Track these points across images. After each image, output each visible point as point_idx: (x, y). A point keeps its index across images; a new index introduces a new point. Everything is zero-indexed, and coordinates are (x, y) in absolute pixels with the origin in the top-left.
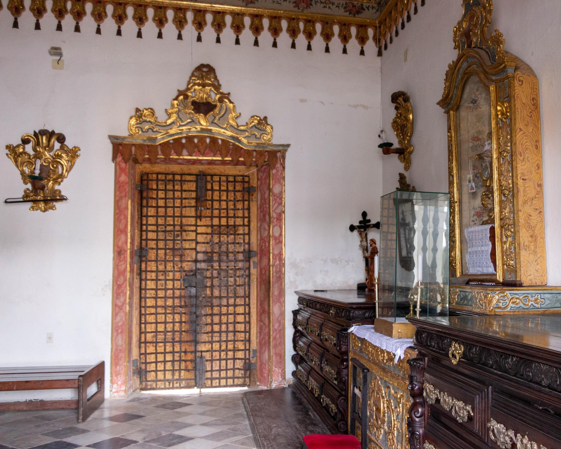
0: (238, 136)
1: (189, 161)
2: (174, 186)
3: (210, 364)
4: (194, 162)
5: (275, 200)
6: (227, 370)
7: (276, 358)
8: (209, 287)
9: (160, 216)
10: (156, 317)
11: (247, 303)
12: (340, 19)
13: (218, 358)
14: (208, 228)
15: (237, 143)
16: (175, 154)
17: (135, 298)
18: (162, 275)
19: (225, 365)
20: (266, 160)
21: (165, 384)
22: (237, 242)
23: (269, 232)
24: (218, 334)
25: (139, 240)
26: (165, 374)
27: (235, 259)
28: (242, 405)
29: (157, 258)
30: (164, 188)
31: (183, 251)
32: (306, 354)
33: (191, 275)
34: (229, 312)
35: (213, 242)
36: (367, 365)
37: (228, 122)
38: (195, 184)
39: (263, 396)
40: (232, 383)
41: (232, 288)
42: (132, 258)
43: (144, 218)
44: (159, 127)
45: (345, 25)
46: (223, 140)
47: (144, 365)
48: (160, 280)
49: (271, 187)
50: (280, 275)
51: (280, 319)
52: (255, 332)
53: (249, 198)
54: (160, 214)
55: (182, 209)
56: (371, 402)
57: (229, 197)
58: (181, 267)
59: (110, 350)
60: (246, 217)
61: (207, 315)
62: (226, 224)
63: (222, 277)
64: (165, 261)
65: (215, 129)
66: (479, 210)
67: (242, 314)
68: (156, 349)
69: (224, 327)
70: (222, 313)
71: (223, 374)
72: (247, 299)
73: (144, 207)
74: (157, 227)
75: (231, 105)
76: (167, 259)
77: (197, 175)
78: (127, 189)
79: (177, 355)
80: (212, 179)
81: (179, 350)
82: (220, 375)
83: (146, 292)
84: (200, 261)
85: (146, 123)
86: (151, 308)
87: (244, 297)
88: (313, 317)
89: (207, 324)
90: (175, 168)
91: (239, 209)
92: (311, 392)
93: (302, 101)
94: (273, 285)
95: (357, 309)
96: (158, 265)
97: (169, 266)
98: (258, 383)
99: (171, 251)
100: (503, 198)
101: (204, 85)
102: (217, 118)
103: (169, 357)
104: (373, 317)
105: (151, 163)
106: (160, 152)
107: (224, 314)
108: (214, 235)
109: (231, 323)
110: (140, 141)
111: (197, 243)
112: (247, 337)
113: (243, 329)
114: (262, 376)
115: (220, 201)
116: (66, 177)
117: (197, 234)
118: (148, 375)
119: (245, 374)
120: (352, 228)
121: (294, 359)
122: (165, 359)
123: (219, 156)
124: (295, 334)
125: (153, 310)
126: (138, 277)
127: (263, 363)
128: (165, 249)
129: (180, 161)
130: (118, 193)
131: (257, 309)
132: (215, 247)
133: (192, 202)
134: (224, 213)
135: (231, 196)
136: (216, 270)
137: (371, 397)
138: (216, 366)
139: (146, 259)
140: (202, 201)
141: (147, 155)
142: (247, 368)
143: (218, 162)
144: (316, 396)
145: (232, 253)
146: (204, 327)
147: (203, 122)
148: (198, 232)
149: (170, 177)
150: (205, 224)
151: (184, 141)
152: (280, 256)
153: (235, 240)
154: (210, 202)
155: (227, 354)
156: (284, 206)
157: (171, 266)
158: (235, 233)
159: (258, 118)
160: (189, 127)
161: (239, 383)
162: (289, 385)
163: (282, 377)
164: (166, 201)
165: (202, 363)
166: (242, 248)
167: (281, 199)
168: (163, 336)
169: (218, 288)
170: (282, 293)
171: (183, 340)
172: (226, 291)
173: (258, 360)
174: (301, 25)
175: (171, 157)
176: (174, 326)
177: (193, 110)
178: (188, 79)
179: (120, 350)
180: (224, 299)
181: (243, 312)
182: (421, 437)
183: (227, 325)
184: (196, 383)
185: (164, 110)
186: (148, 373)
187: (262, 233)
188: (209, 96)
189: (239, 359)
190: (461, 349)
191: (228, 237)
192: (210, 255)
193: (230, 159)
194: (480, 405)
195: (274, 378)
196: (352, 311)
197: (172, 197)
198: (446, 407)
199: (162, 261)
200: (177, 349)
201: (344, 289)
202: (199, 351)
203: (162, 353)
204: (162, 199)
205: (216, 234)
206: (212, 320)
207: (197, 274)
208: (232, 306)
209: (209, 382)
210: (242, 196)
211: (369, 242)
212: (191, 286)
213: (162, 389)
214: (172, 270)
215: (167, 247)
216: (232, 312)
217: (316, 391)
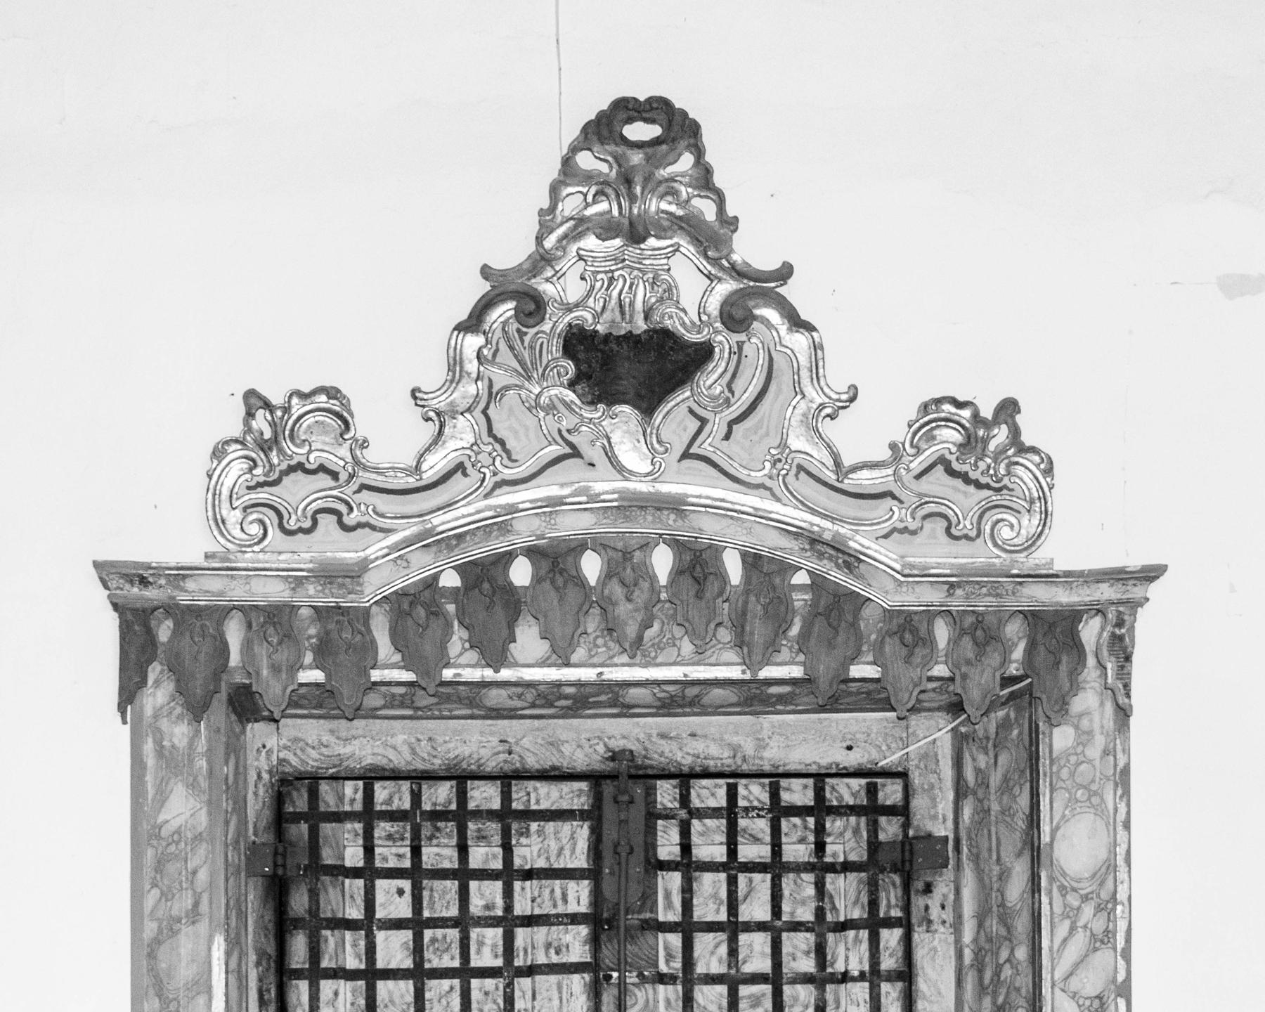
0: (844, 530)
2: (463, 849)
20: (1013, 670)
30: (407, 864)
37: (783, 445)
38: (583, 832)
53: (907, 908)
55: (510, 985)
57: (786, 907)
73: (298, 974)
77: (595, 778)
78: (203, 876)
80: (685, 800)
85: (299, 475)
91: (845, 978)
101: (635, 233)
102: (718, 424)
115: (733, 928)
123: (731, 656)
129: (496, 697)
133: (568, 938)
140: (630, 935)
147: (633, 456)
149: (440, 795)
151: (521, 573)
154: (675, 940)
156: (1127, 955)
160: (555, 491)
164: (418, 938)
177: (572, 385)
193: (797, 672)
197: (454, 912)
204: (398, 924)
210: (865, 899)
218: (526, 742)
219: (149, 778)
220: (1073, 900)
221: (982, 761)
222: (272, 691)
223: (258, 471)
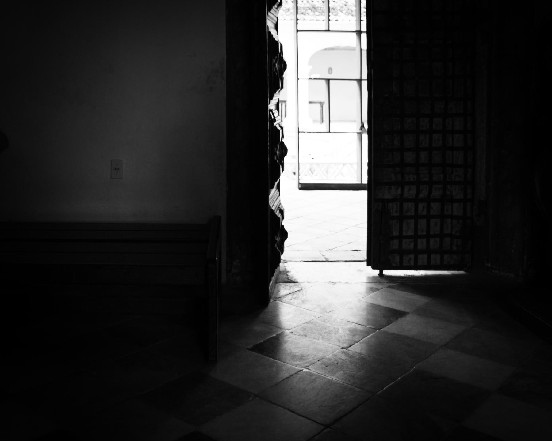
13: (412, 213)
138: (409, 229)
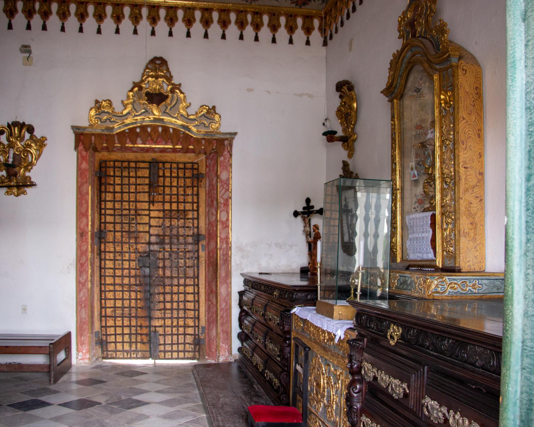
0: (188, 125)
1: (142, 149)
2: (129, 173)
3: (163, 338)
4: (148, 150)
5: (223, 186)
6: (178, 344)
7: (223, 335)
8: (162, 268)
9: (117, 201)
10: (115, 294)
11: (196, 283)
12: (287, 10)
13: (170, 333)
14: (160, 213)
15: (187, 132)
16: (130, 143)
17: (95, 276)
18: (119, 255)
19: (176, 340)
21: (123, 354)
22: (187, 225)
23: (217, 217)
24: (170, 312)
25: (98, 223)
26: (123, 346)
27: (185, 242)
28: (193, 376)
29: (114, 240)
30: (120, 175)
31: (138, 233)
32: (251, 332)
33: (144, 256)
34: (180, 291)
35: (165, 226)
36: (308, 344)
37: (179, 111)
38: (148, 171)
39: (211, 368)
40: (183, 356)
41: (182, 269)
42: (92, 239)
43: (103, 203)
44: (116, 118)
45: (291, 16)
46: (174, 129)
47: (105, 336)
48: (117, 260)
49: (219, 174)
50: (227, 258)
51: (226, 299)
52: (204, 310)
54: (117, 199)
55: (136, 195)
56: (311, 378)
57: (179, 184)
58: (136, 248)
59: (75, 322)
60: (195, 203)
61: (160, 293)
62: (176, 209)
63: (173, 259)
64: (122, 243)
65: (166, 118)
66: (420, 197)
67: (192, 293)
68: (115, 323)
69: (175, 305)
70: (173, 292)
71: (175, 348)
72: (196, 280)
73: (103, 192)
74: (115, 211)
75: (182, 95)
76: (123, 241)
77: (150, 162)
78: (88, 176)
79: (133, 329)
80: (164, 166)
81: (135, 324)
82: (172, 348)
83: (105, 270)
84: (153, 244)
85: (104, 113)
86: (110, 286)
87: (194, 278)
88: (258, 298)
89: (160, 302)
90: (131, 156)
91: (188, 195)
92: (256, 367)
93: (250, 90)
94: (220, 267)
95: (299, 291)
96: (116, 247)
97: (126, 248)
98: (207, 357)
99: (127, 233)
100: (445, 186)
101: (157, 77)
102: (169, 108)
103: (126, 331)
104: (315, 299)
105: (109, 151)
106: (117, 141)
107: (175, 293)
108: (165, 219)
109: (181, 302)
110: (99, 131)
111: (150, 226)
112: (196, 314)
113: (192, 308)
114: (210, 351)
115: (171, 187)
116: (35, 165)
117: (150, 218)
118: (108, 346)
119: (195, 349)
120: (296, 214)
121: (239, 336)
122: (123, 332)
123: (171, 144)
124: (241, 313)
125: (112, 288)
126: (98, 257)
127: (211, 339)
128: (122, 232)
129: (134, 149)
130: (80, 179)
131: (205, 289)
132: (167, 230)
133: (145, 187)
134: (174, 198)
135: (181, 182)
136: (167, 251)
137: (312, 373)
138: (168, 340)
139: (105, 240)
140: (155, 187)
141: (106, 143)
142: (197, 343)
143: (169, 150)
144: (260, 370)
145: (182, 236)
146: (157, 304)
147: (156, 112)
148: (151, 216)
149: (126, 164)
150: (157, 209)
151: (138, 130)
152: (227, 240)
153: (185, 224)
154: (162, 188)
155: (178, 330)
156: (231, 192)
157: (127, 248)
158: (185, 217)
159: (207, 108)
160: (143, 117)
161: (189, 356)
162: (235, 360)
163: (228, 353)
164: (122, 187)
165: (156, 337)
166: (192, 232)
167: (228, 185)
168: (121, 312)
169: (169, 269)
170: (228, 275)
171: (138, 315)
172: (177, 272)
173: (207, 337)
174: (249, 17)
175: (127, 145)
176: (130, 302)
177: (147, 101)
178: (142, 71)
179: (84, 322)
180: (175, 279)
181: (193, 292)
182: (359, 411)
183: (178, 304)
184: (151, 354)
185: (120, 101)
186: (108, 344)
187: (210, 218)
188: (162, 87)
189: (189, 334)
190: (399, 331)
191: (178, 221)
192: (162, 237)
193: (180, 147)
194: (416, 383)
195: (221, 353)
196: (295, 294)
197: (127, 183)
198: (383, 384)
199: (119, 243)
200: (133, 323)
201: (288, 272)
202: (153, 326)
203: (120, 327)
204: (119, 185)
205: (168, 218)
206: (164, 299)
207: (151, 255)
208: (182, 285)
209: (163, 354)
211: (312, 227)
212: (145, 266)
213: (121, 358)
214: (128, 251)
215: (124, 230)
216: (183, 291)
217: (260, 367)
218: (139, 156)
219: (80, 160)
220: (223, 184)
221: (210, 162)
222: (99, 148)
223: (97, 112)
